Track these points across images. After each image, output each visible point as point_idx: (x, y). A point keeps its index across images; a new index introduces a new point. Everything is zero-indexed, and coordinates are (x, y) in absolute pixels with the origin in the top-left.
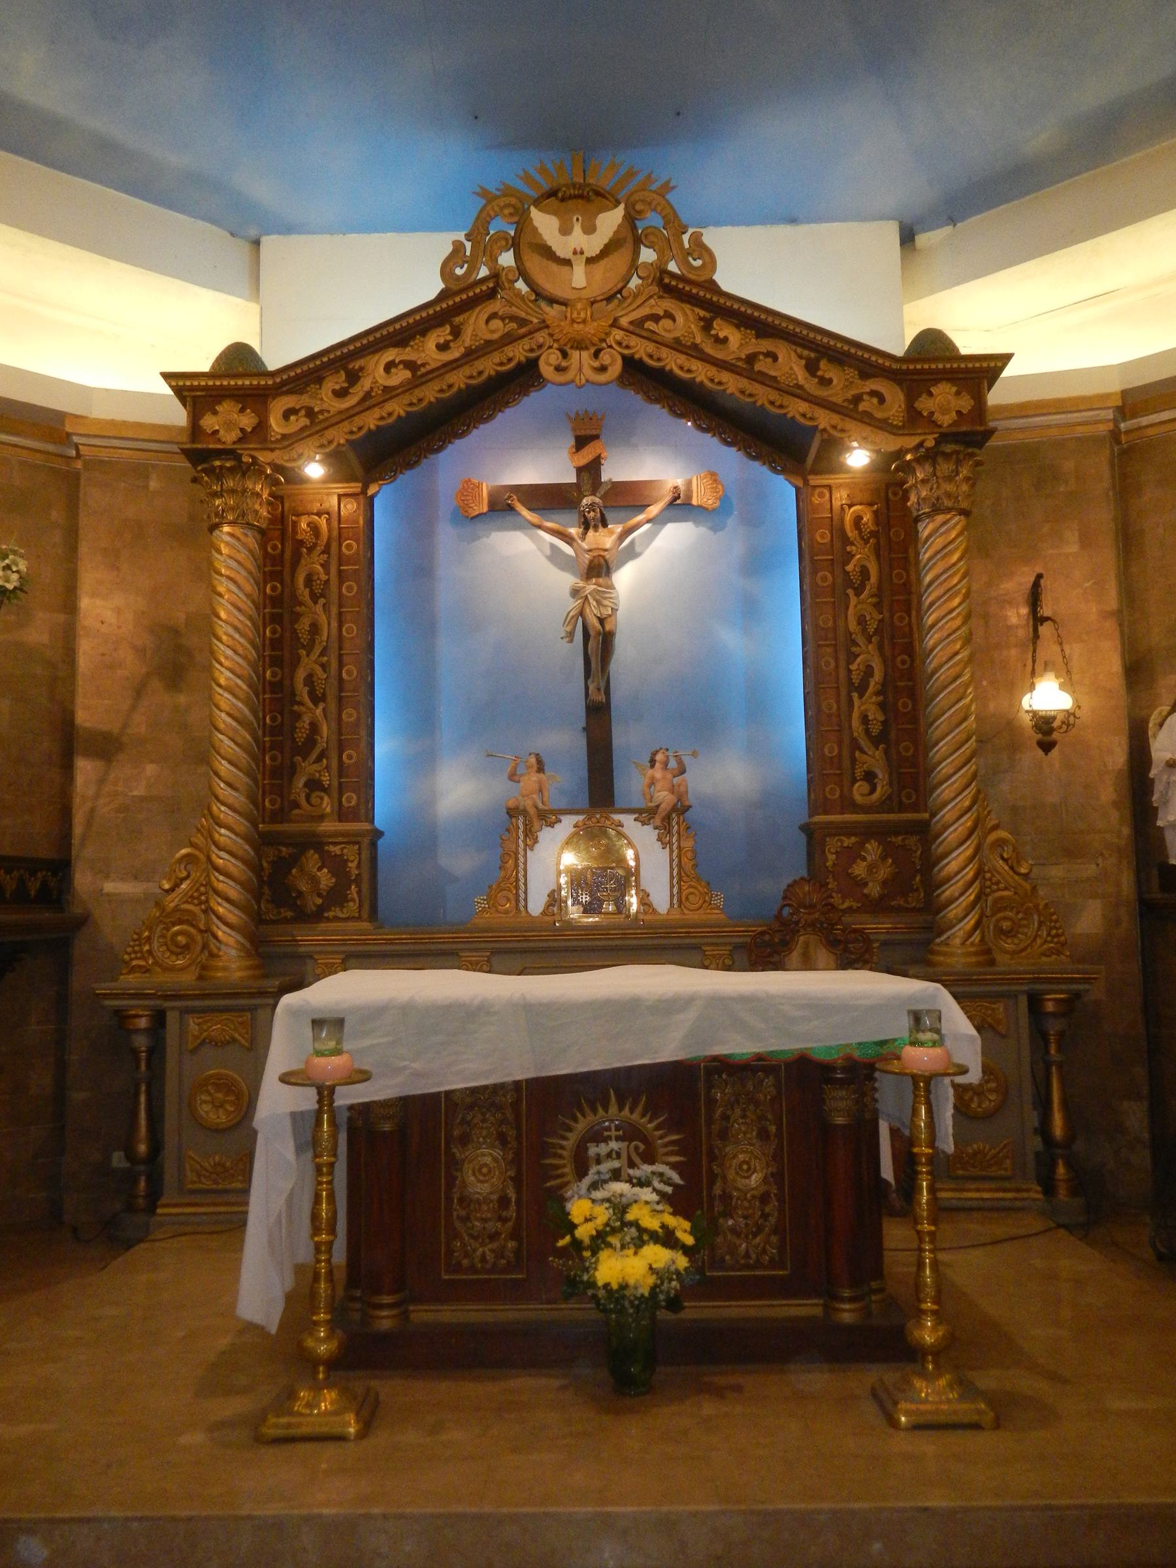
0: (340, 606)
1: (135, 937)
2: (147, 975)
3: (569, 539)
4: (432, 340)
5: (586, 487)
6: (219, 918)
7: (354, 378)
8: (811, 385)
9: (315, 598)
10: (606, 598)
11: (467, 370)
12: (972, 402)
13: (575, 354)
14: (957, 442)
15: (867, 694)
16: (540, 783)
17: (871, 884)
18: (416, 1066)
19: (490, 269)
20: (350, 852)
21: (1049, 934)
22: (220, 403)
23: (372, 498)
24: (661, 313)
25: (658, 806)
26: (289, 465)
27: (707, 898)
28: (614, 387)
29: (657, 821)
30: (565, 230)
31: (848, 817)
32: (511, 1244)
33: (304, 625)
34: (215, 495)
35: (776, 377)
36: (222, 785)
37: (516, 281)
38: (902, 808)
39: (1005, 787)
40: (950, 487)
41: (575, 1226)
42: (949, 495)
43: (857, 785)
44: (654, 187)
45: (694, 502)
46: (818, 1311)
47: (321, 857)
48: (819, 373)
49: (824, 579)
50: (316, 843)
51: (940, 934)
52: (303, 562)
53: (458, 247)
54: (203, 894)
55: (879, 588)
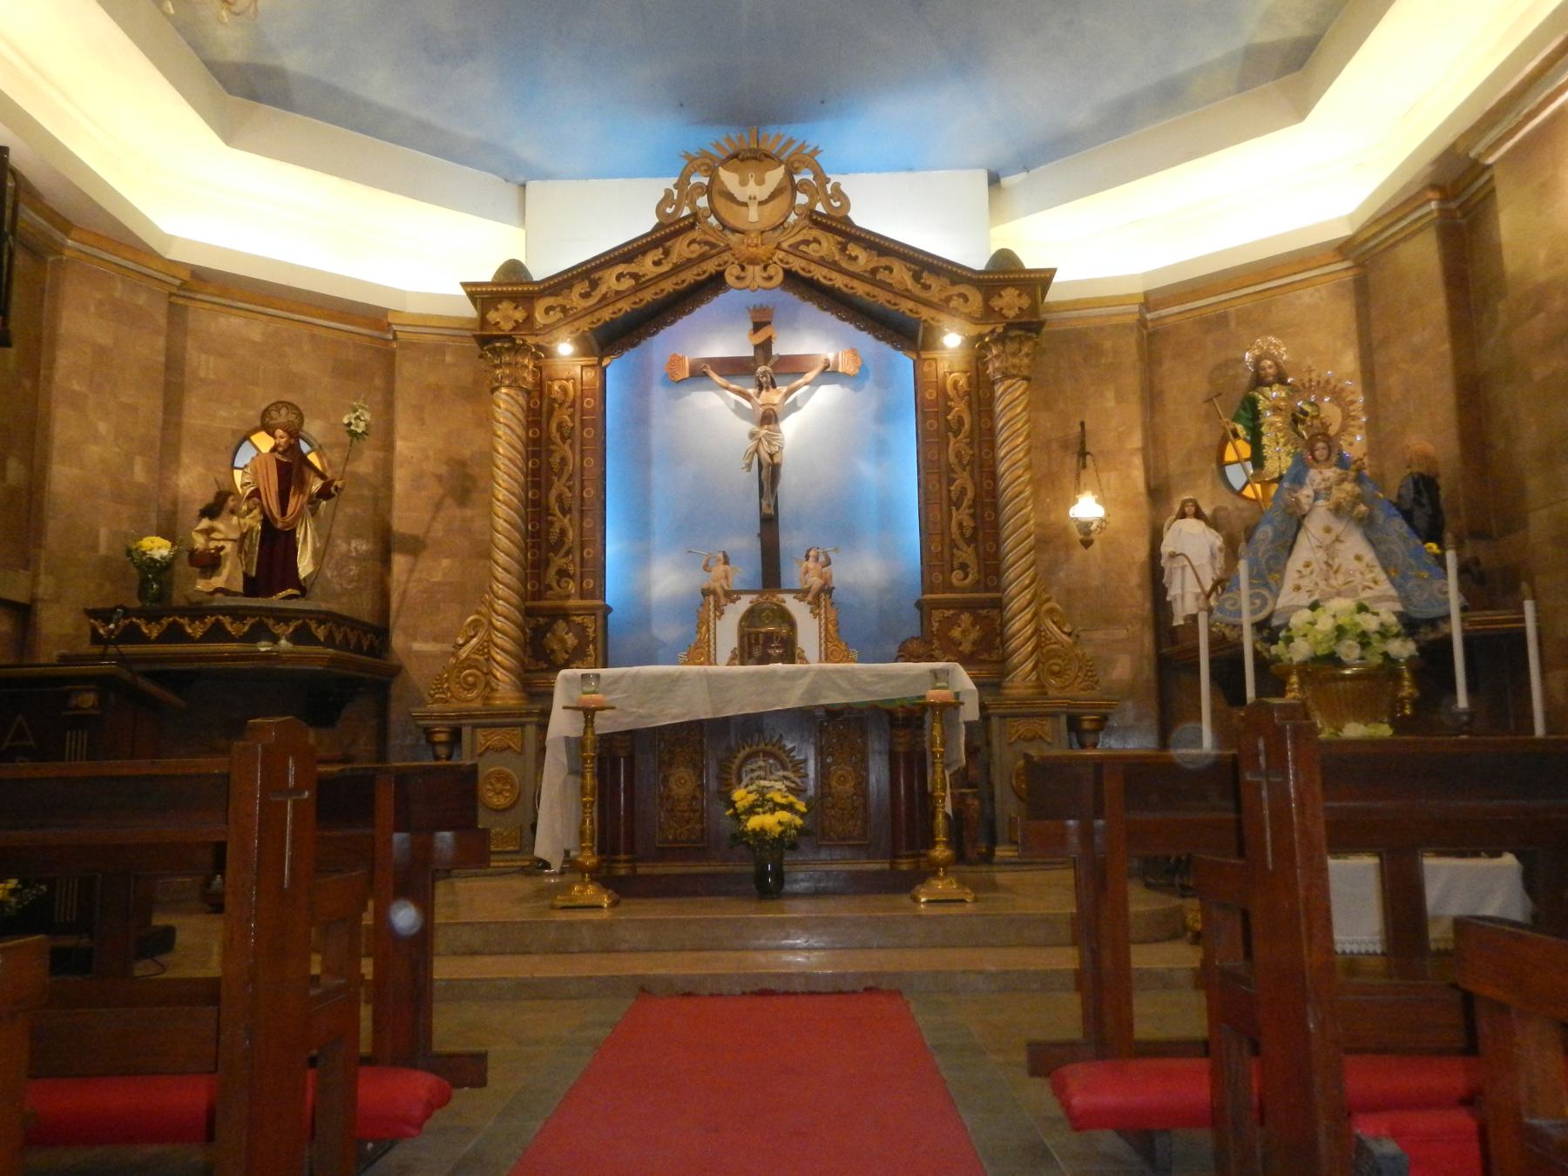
0: (582, 445)
3: (748, 397)
4: (649, 259)
5: (761, 359)
6: (498, 663)
7: (594, 285)
9: (564, 439)
11: (674, 279)
12: (1030, 301)
13: (750, 268)
14: (1020, 329)
20: (589, 621)
21: (1086, 675)
22: (500, 302)
24: (811, 239)
28: (778, 289)
29: (810, 598)
30: (743, 183)
32: (698, 826)
33: (555, 459)
34: (496, 367)
35: (891, 284)
38: (987, 589)
39: (1062, 574)
40: (1016, 361)
41: (735, 802)
42: (1014, 366)
44: (807, 151)
45: (840, 370)
46: (887, 866)
48: (922, 281)
49: (931, 426)
50: (565, 615)
51: (1008, 675)
52: (556, 414)
53: (668, 193)
54: (485, 648)
55: (972, 432)
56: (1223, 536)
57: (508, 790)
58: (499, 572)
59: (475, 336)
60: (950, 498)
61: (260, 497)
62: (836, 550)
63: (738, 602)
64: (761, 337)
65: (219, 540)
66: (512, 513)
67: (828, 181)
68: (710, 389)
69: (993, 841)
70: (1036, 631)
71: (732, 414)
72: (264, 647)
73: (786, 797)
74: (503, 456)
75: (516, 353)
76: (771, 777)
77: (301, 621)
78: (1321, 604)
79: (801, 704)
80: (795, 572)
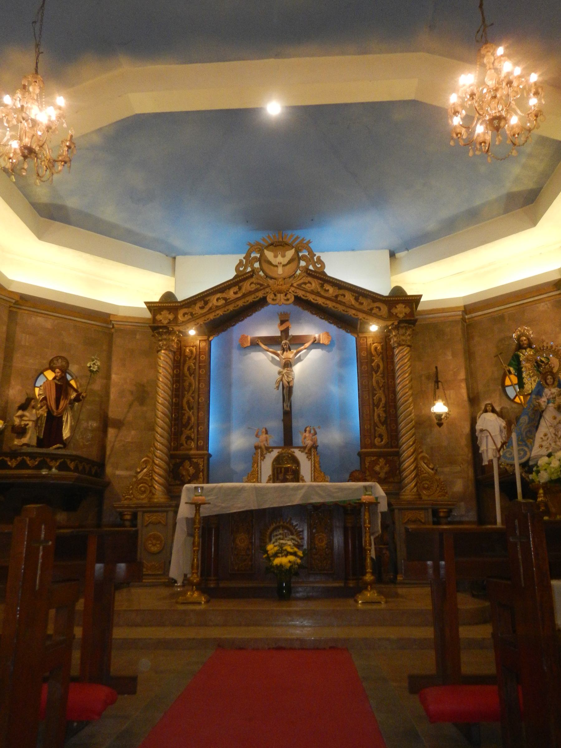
0: (199, 377)
1: (127, 488)
2: (131, 501)
3: (278, 355)
4: (231, 292)
7: (206, 303)
8: (357, 305)
9: (191, 375)
10: (290, 375)
11: (243, 300)
12: (410, 310)
13: (278, 295)
14: (406, 323)
15: (380, 407)
16: (266, 438)
17: (381, 474)
18: (223, 505)
19: (251, 268)
20: (200, 461)
21: (441, 489)
22: (162, 311)
23: (210, 341)
24: (307, 282)
25: (307, 446)
26: (184, 331)
27: (324, 478)
28: (292, 305)
29: (306, 451)
30: (276, 256)
31: (372, 450)
32: (250, 563)
33: (186, 384)
34: (160, 340)
35: (344, 303)
36: (159, 436)
37: (260, 272)
38: (392, 447)
39: (428, 440)
40: (404, 338)
42: (403, 340)
43: (377, 438)
44: (305, 242)
45: (321, 342)
47: (191, 463)
49: (364, 368)
50: (189, 458)
51: (403, 489)
52: (187, 362)
53: (241, 261)
56: (506, 421)
57: (159, 544)
58: (158, 437)
59: (151, 327)
60: (374, 404)
61: (46, 400)
62: (319, 428)
63: (272, 453)
64: (284, 327)
65: (26, 421)
66: (165, 409)
67: (315, 255)
68: (260, 351)
69: (396, 572)
70: (416, 467)
71: (270, 363)
72: (44, 472)
73: (292, 549)
74: (162, 382)
75: (169, 334)
76: (286, 539)
77: (62, 460)
78: (553, 454)
79: (300, 502)
80: (299, 439)
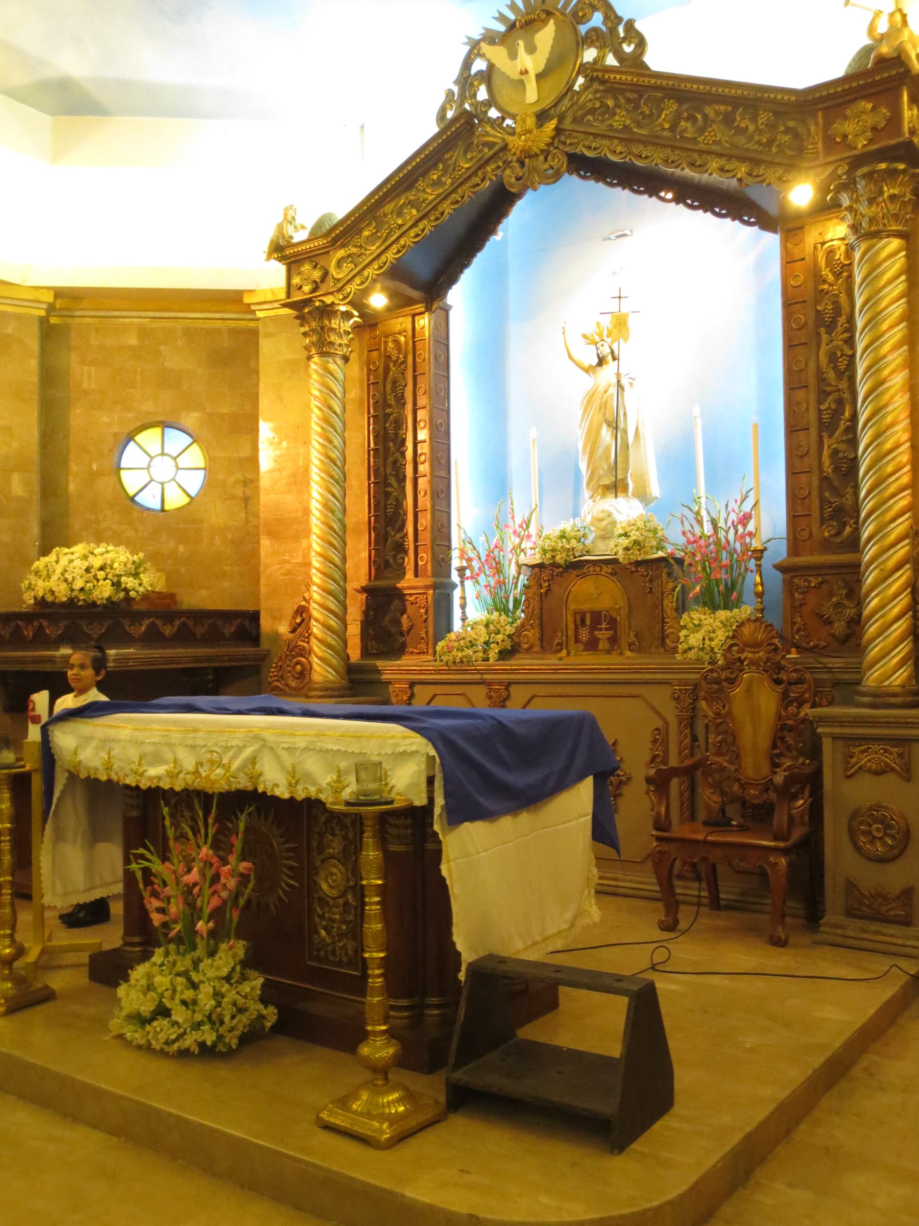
53: (450, 93)
